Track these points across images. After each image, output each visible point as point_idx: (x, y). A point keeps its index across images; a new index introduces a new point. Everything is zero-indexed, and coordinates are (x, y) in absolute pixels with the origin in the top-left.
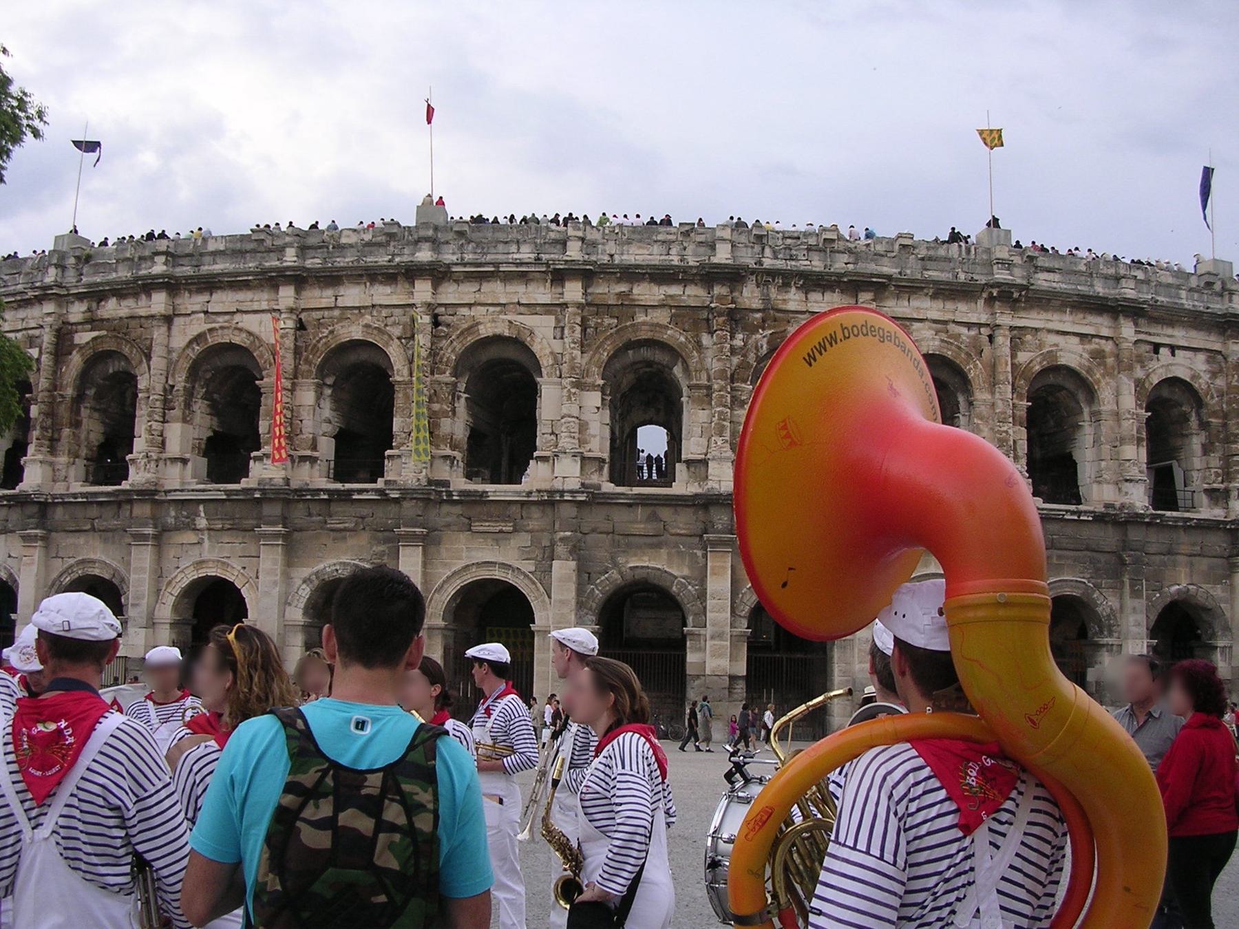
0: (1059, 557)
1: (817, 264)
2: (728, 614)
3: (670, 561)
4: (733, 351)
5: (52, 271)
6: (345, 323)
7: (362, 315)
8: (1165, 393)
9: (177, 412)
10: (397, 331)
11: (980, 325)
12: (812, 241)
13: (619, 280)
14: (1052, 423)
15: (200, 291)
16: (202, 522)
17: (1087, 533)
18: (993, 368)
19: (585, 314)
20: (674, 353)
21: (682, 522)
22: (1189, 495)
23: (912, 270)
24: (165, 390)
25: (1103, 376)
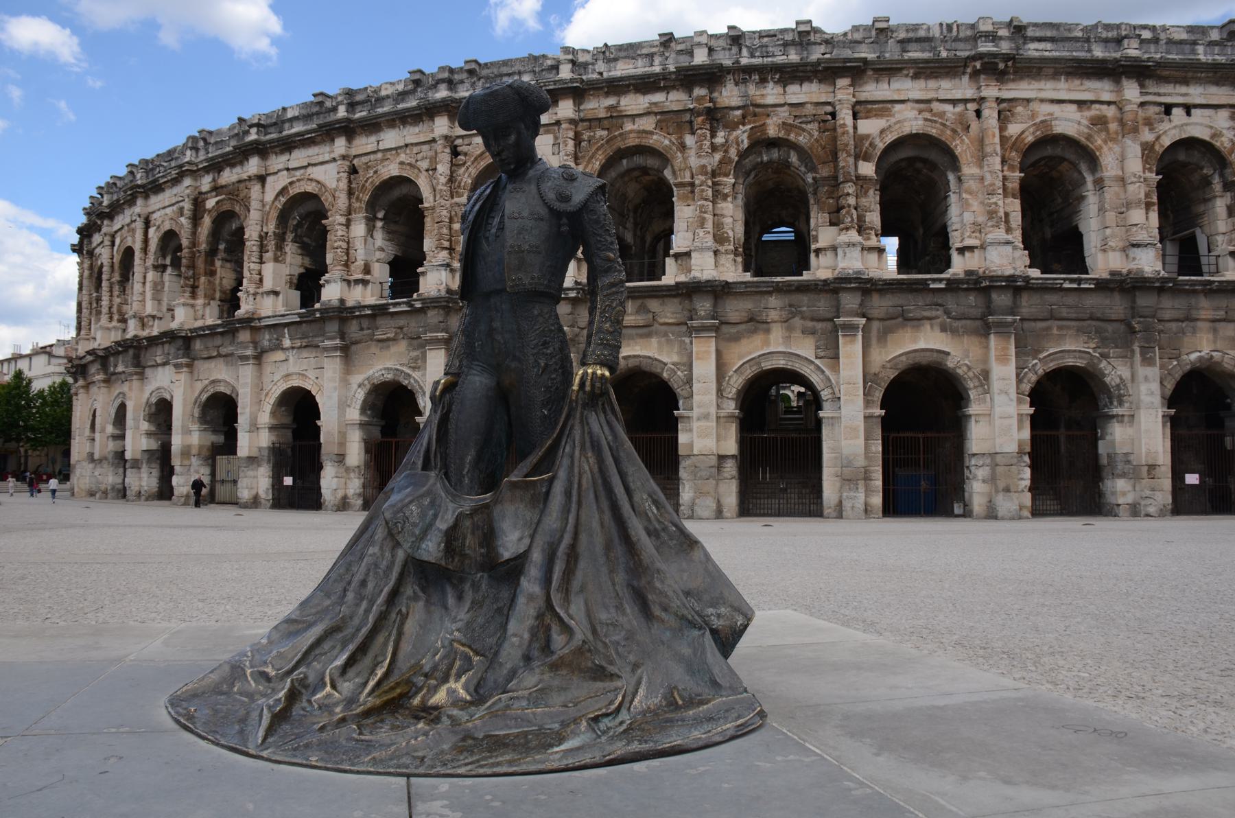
0: (1060, 328)
1: (793, 57)
2: (714, 397)
3: (660, 349)
4: (714, 148)
5: (188, 153)
6: (386, 163)
7: (398, 154)
8: (1182, 156)
9: (269, 255)
10: (424, 165)
11: (965, 101)
12: (789, 37)
13: (607, 94)
14: (1060, 200)
15: (282, 152)
16: (287, 343)
17: (1092, 301)
18: (981, 142)
19: (579, 129)
20: (663, 157)
21: (668, 312)
22: (1213, 260)
23: (891, 52)
24: (261, 237)
25: (1105, 142)
